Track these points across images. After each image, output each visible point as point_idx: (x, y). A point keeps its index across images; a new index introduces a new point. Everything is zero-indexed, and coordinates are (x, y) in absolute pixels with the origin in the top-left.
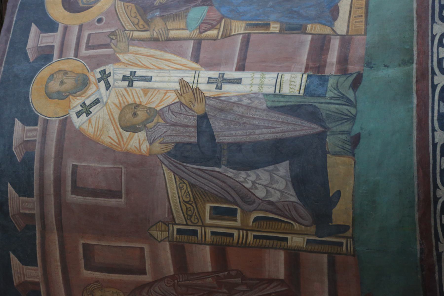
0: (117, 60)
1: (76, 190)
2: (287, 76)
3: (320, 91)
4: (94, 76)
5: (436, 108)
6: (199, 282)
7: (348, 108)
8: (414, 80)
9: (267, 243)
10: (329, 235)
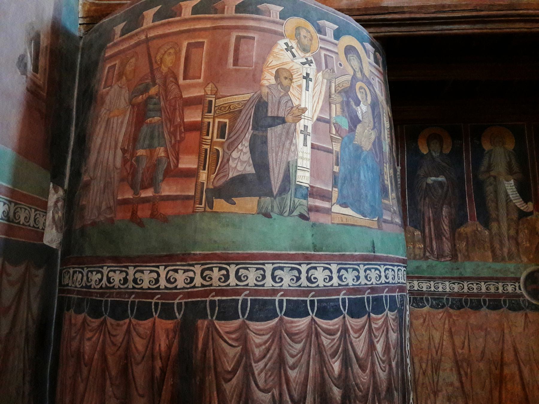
0: (318, 71)
1: (239, 39)
2: (308, 174)
3: (299, 195)
4: (309, 56)
5: (287, 265)
6: (177, 113)
7: (288, 211)
8: (304, 252)
9: (202, 158)
10: (206, 197)
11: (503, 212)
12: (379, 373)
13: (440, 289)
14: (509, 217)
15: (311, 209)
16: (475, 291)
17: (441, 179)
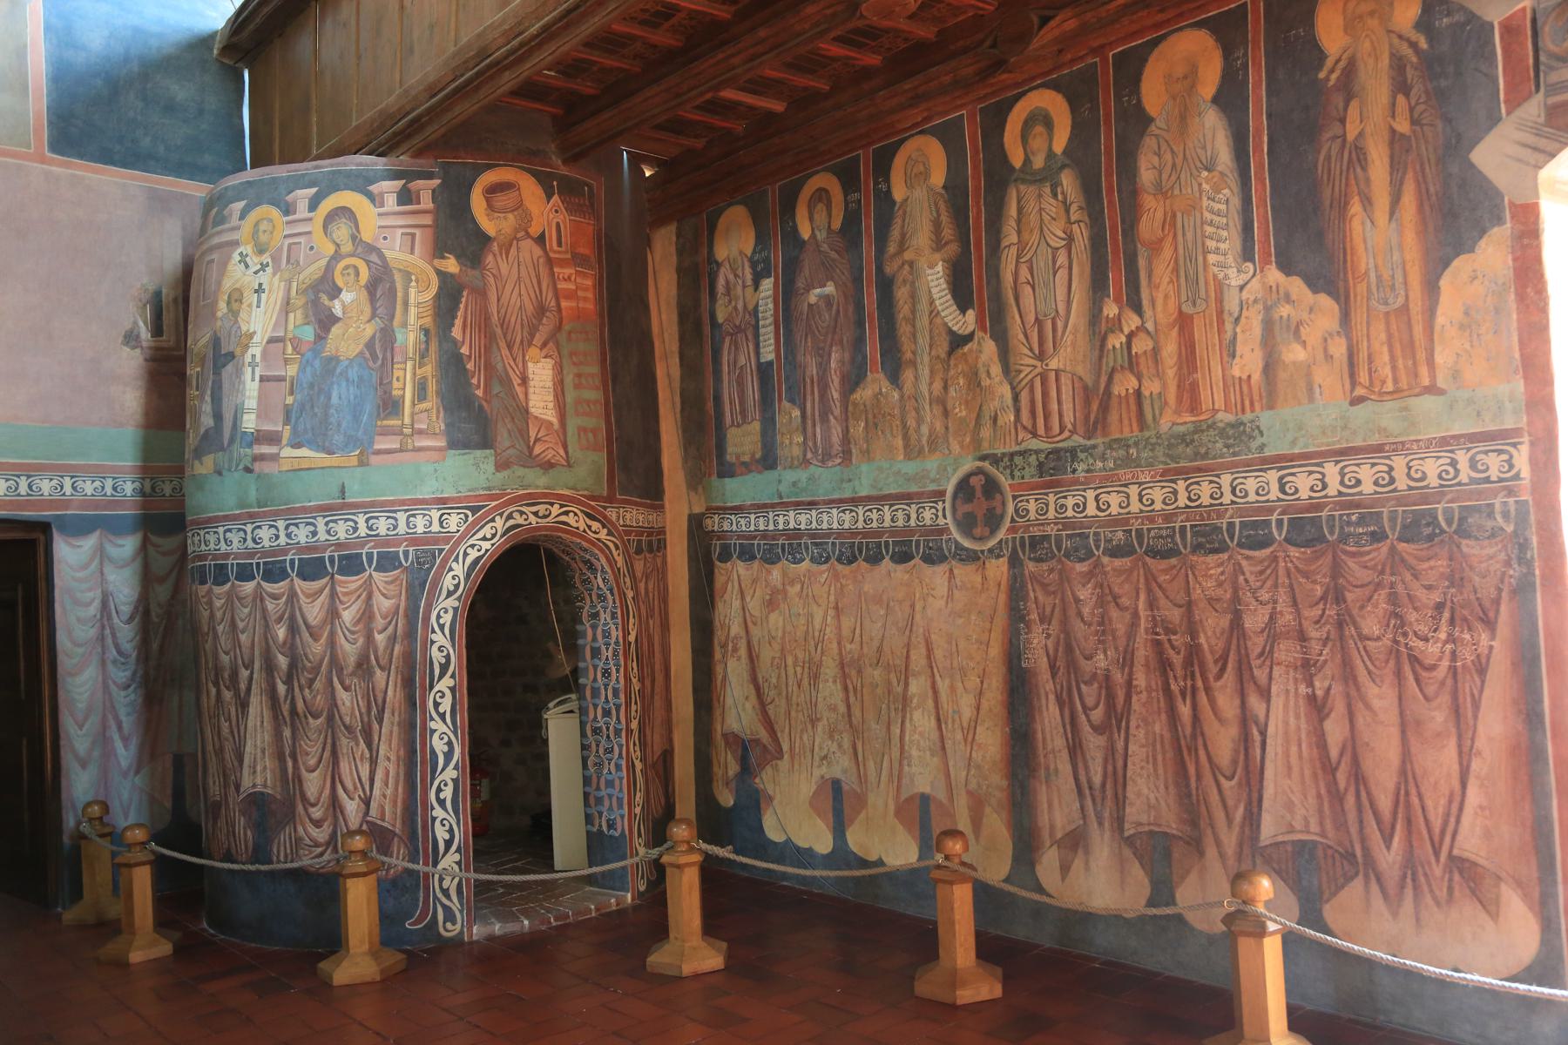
0: (274, 274)
2: (253, 416)
3: (244, 444)
11: (923, 341)
12: (341, 646)
13: (825, 526)
14: (933, 353)
15: (256, 458)
16: (875, 525)
17: (830, 289)
